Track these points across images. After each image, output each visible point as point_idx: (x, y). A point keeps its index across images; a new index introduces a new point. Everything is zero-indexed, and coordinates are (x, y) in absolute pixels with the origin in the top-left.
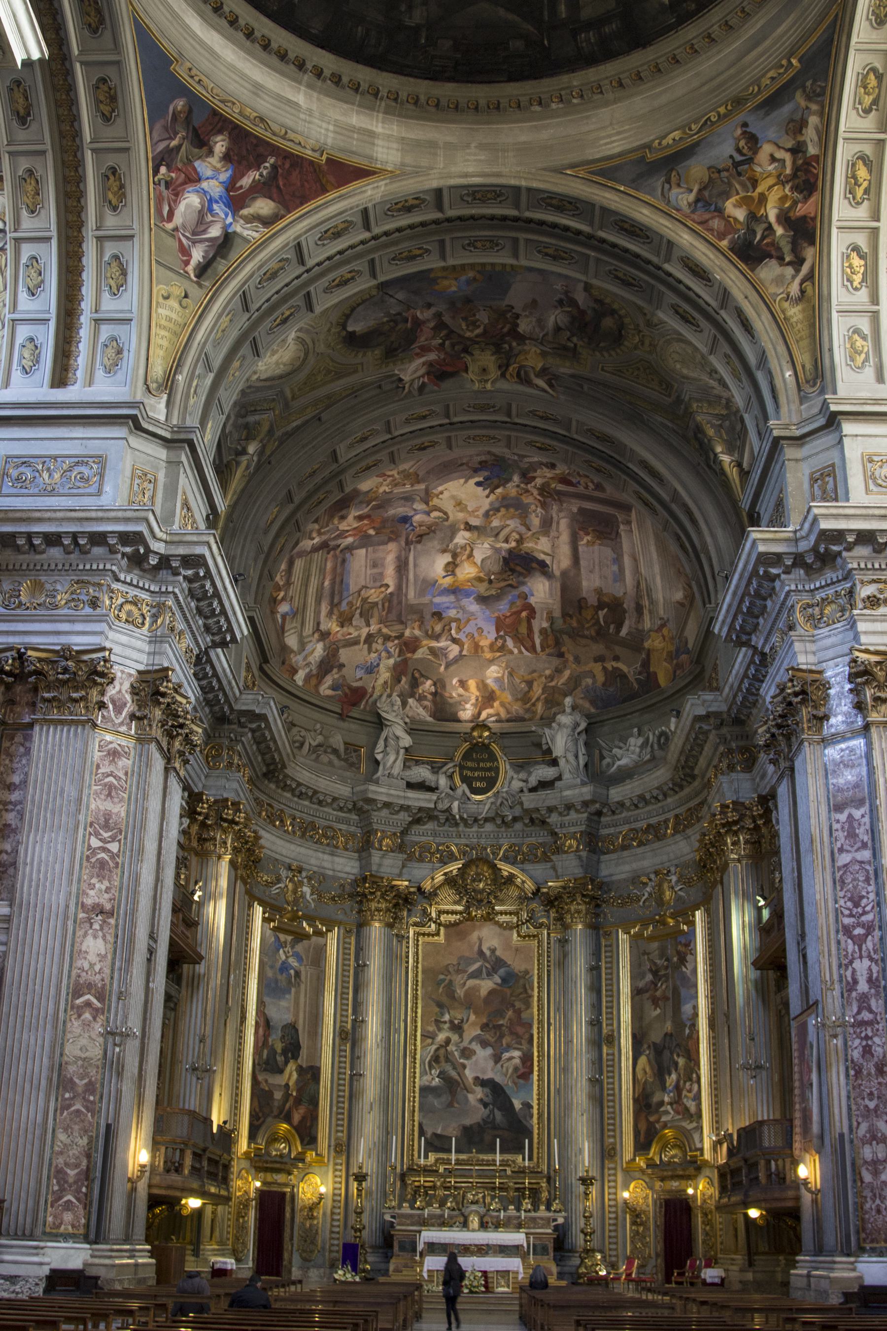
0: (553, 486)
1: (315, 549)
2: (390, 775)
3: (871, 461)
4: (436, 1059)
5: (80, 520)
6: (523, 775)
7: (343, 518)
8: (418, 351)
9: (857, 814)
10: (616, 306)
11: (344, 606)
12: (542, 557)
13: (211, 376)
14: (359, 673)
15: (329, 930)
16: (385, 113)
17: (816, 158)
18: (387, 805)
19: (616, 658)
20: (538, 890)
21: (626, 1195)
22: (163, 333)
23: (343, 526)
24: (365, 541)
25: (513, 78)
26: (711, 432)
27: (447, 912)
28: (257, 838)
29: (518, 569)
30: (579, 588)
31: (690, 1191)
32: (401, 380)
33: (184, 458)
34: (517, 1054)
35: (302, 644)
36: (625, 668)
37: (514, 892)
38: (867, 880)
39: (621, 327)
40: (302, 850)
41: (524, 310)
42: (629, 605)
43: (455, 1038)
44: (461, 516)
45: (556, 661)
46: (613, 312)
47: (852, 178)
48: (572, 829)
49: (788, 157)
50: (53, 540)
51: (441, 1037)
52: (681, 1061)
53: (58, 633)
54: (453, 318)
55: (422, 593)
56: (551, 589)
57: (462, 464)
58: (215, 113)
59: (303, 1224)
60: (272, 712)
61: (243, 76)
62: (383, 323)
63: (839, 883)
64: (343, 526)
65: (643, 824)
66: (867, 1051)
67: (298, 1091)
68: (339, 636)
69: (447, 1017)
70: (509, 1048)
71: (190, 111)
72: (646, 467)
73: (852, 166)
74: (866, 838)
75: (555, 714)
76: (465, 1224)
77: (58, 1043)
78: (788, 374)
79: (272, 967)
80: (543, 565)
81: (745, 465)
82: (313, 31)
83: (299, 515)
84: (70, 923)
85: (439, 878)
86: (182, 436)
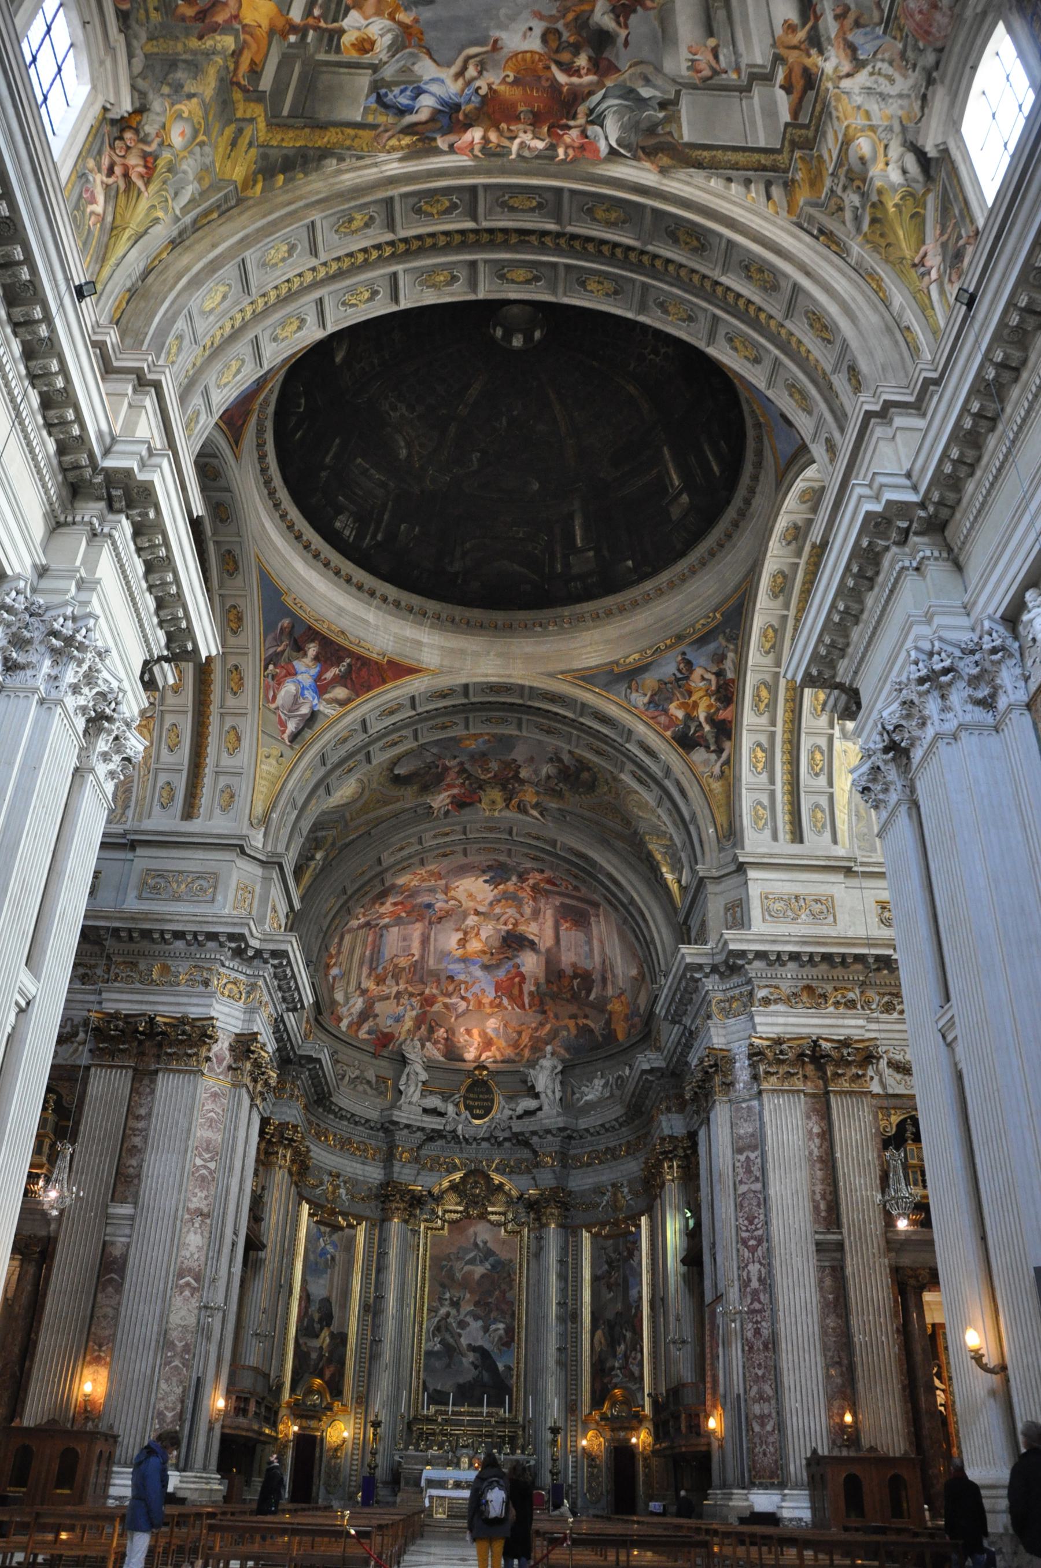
1: (360, 927)
2: (410, 1103)
3: (767, 898)
4: (438, 1329)
5: (200, 922)
6: (513, 1106)
7: (382, 904)
9: (752, 1156)
11: (380, 970)
12: (531, 937)
13: (296, 812)
14: (389, 1022)
15: (359, 1224)
16: (431, 627)
17: (733, 681)
18: (408, 1126)
19: (586, 1017)
20: (522, 1195)
21: (584, 1443)
22: (264, 782)
23: (382, 910)
24: (398, 921)
26: (659, 857)
27: (451, 1211)
28: (309, 1151)
30: (559, 962)
31: (634, 1440)
33: (274, 876)
34: (501, 1326)
35: (347, 999)
36: (592, 1025)
37: (502, 1198)
38: (759, 1205)
39: (595, 779)
40: (341, 1160)
42: (596, 976)
43: (453, 1312)
44: (471, 904)
45: (540, 1017)
46: (589, 769)
47: (757, 697)
48: (549, 1149)
49: (713, 678)
50: (179, 935)
51: (443, 1311)
52: (628, 1335)
53: (178, 1004)
55: (439, 961)
58: (310, 628)
59: (329, 1462)
60: (325, 1057)
61: (331, 602)
63: (739, 1206)
65: (602, 1147)
66: (757, 1332)
67: (331, 1352)
69: (447, 1296)
70: (495, 1321)
71: (293, 627)
73: (757, 689)
74: (758, 1174)
75: (538, 1058)
76: (457, 1465)
77: (164, 1315)
78: (711, 830)
79: (314, 1252)
81: (683, 882)
83: (350, 904)
84: (178, 1222)
85: (446, 1184)
86: (275, 860)
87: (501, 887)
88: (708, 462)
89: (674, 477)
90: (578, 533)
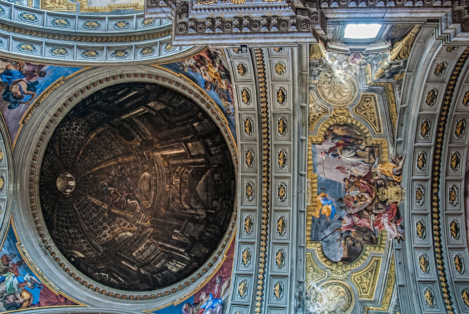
8: (377, 228)
10: (325, 129)
17: (194, 58)
25: (233, 177)
32: (396, 238)
39: (338, 125)
41: (347, 173)
46: (328, 129)
54: (353, 208)
62: (345, 243)
71: (189, 304)
72: (432, 101)
82: (207, 251)
88: (130, 97)
89: (139, 111)
90: (175, 152)
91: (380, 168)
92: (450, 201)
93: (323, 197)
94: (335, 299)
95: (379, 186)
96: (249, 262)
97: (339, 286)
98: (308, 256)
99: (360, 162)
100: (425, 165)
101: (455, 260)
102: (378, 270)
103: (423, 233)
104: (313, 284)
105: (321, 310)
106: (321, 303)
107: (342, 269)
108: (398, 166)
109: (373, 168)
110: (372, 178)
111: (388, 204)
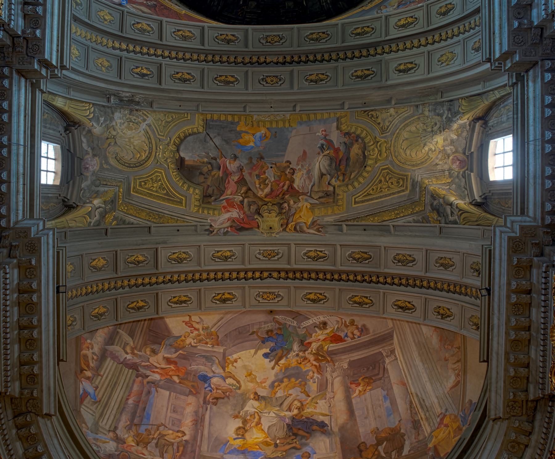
0: (326, 347)
7: (154, 352)
11: (142, 429)
12: (321, 418)
23: (153, 360)
24: (169, 385)
29: (301, 432)
44: (251, 385)
56: (331, 444)
57: (253, 333)
64: (153, 360)
68: (133, 449)
80: (322, 425)
87: (282, 361)
91: (305, 206)
92: (261, 293)
93: (265, 135)
94: (132, 146)
95: (280, 205)
96: (177, 38)
97: (147, 152)
98: (186, 116)
99: (313, 181)
100: (309, 260)
101: (185, 296)
102: (169, 203)
103: (219, 258)
104: (150, 120)
105: (116, 127)
106: (126, 127)
107: (170, 157)
108: (308, 229)
109: (305, 197)
110: (291, 196)
111: (255, 217)
